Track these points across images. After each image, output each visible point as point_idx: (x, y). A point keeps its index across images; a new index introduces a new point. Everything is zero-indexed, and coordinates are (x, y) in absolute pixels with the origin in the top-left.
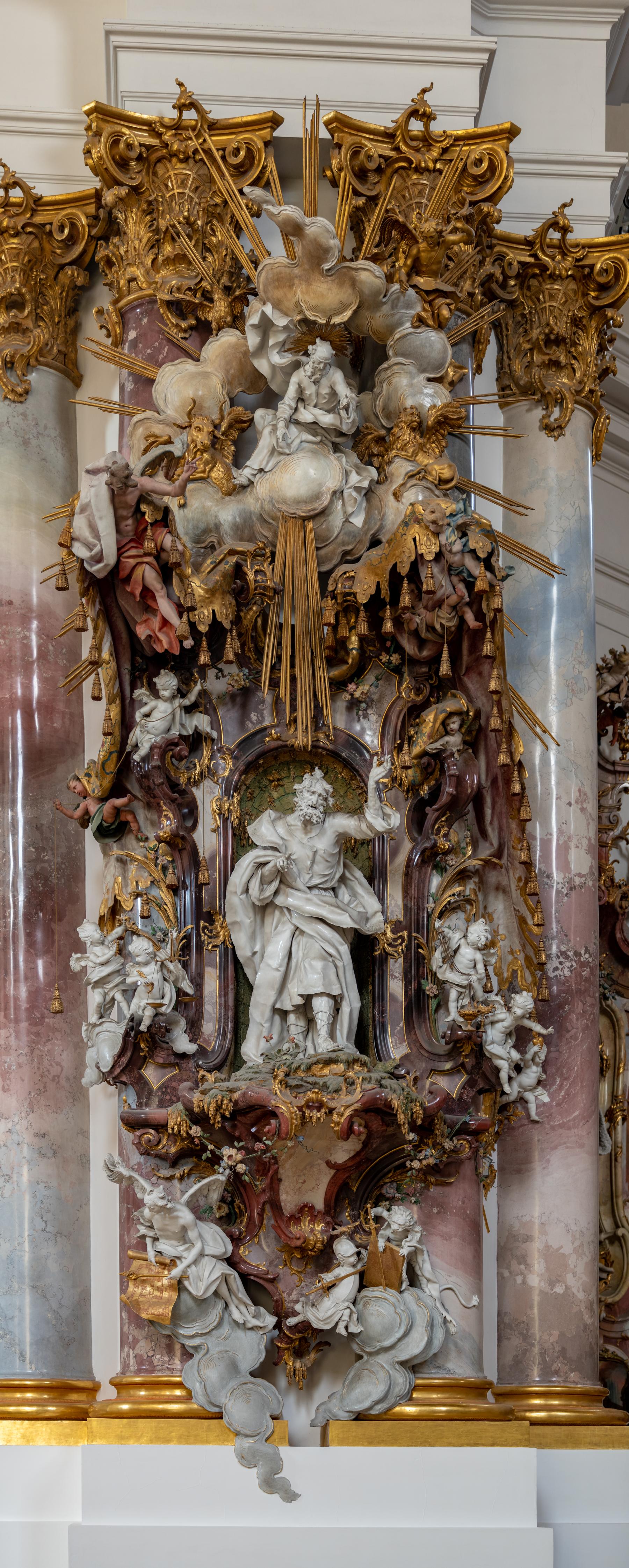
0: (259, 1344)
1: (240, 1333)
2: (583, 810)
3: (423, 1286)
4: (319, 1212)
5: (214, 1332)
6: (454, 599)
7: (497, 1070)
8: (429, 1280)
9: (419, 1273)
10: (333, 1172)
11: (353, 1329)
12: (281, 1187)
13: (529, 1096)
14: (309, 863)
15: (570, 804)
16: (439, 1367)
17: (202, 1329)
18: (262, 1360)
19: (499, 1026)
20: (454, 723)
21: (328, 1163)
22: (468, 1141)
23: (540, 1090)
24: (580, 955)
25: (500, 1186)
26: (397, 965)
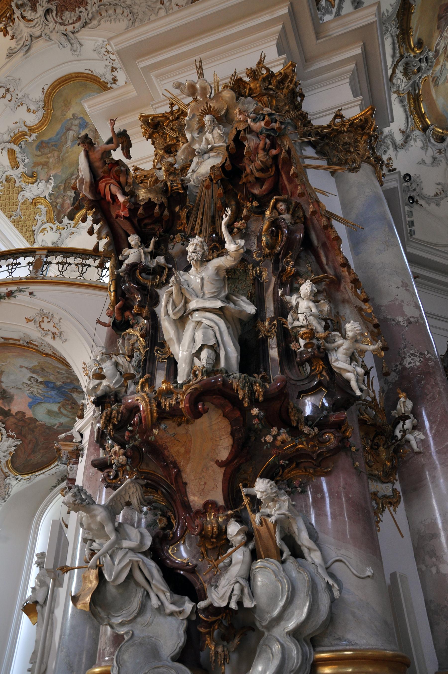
0: (178, 629)
1: (160, 619)
2: (406, 290)
3: (306, 555)
4: (221, 507)
5: (139, 619)
6: (261, 144)
7: (348, 382)
8: (309, 549)
9: (299, 543)
10: (223, 470)
11: (248, 604)
12: (188, 490)
13: (409, 437)
14: (200, 286)
15: (398, 288)
16: (340, 639)
17: (126, 617)
18: (181, 644)
19: (341, 350)
20: (281, 206)
21: (217, 462)
22: (332, 433)
23: (416, 433)
24: (424, 354)
25: (406, 502)
26: (274, 341)
